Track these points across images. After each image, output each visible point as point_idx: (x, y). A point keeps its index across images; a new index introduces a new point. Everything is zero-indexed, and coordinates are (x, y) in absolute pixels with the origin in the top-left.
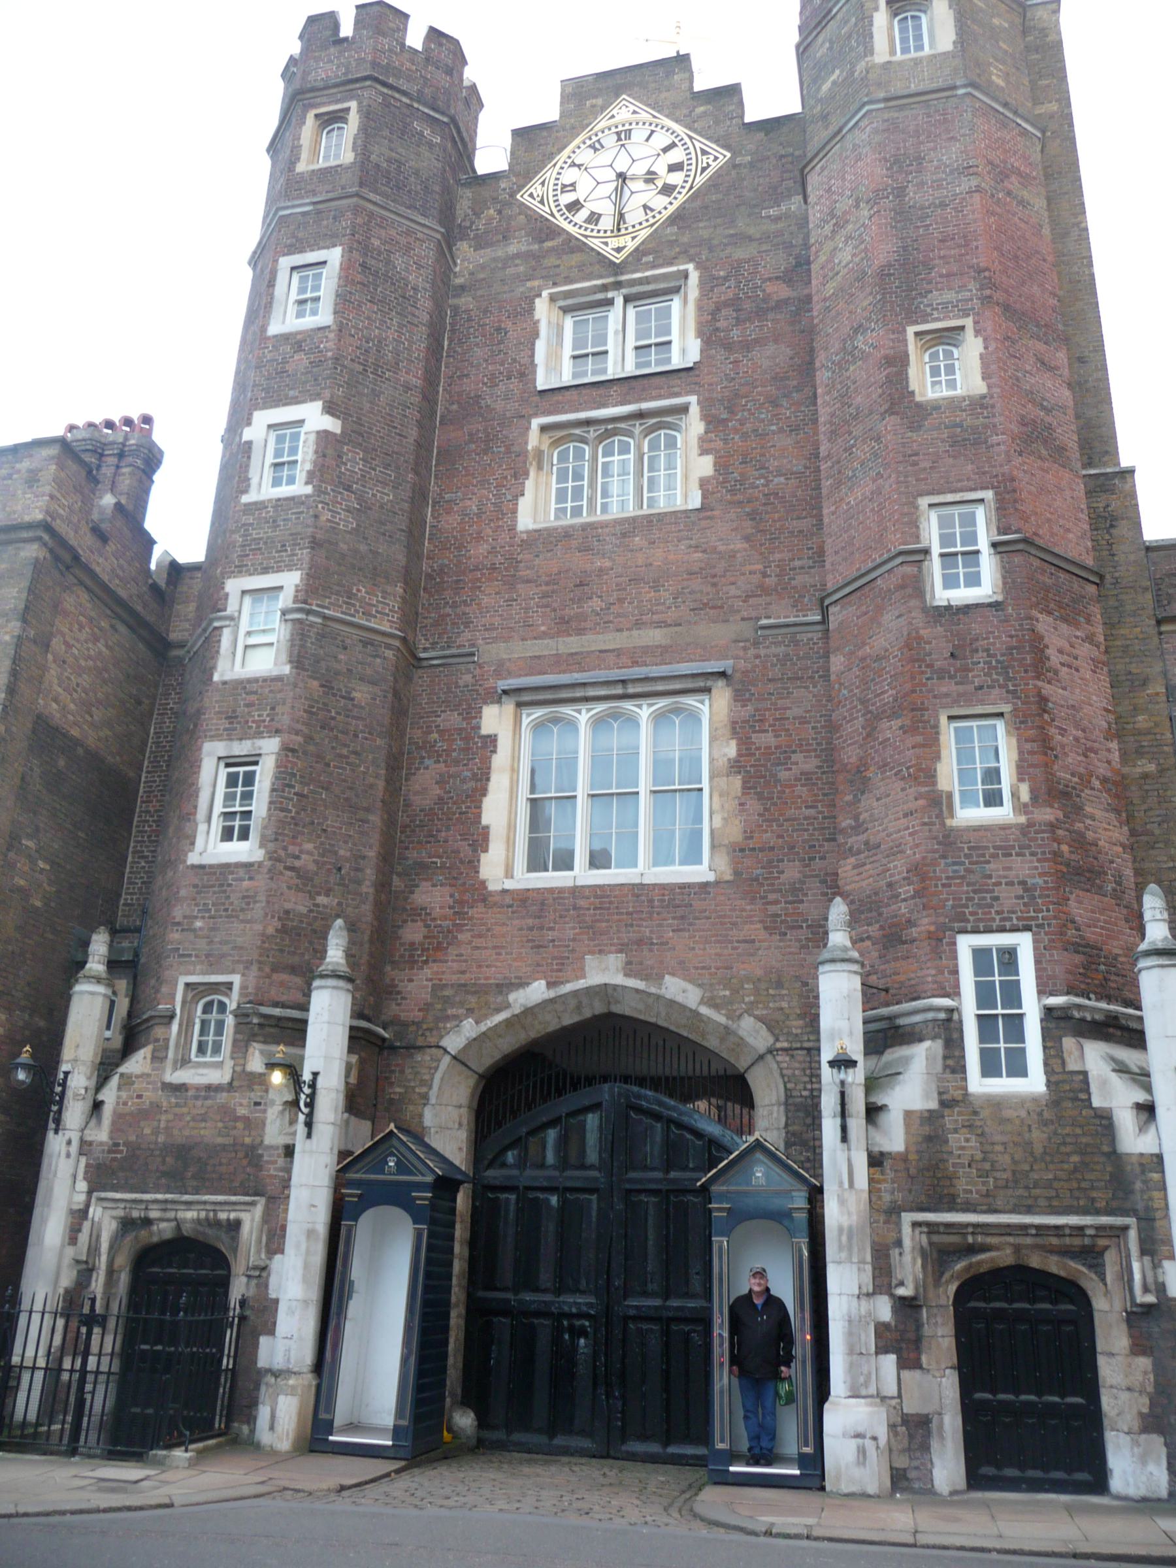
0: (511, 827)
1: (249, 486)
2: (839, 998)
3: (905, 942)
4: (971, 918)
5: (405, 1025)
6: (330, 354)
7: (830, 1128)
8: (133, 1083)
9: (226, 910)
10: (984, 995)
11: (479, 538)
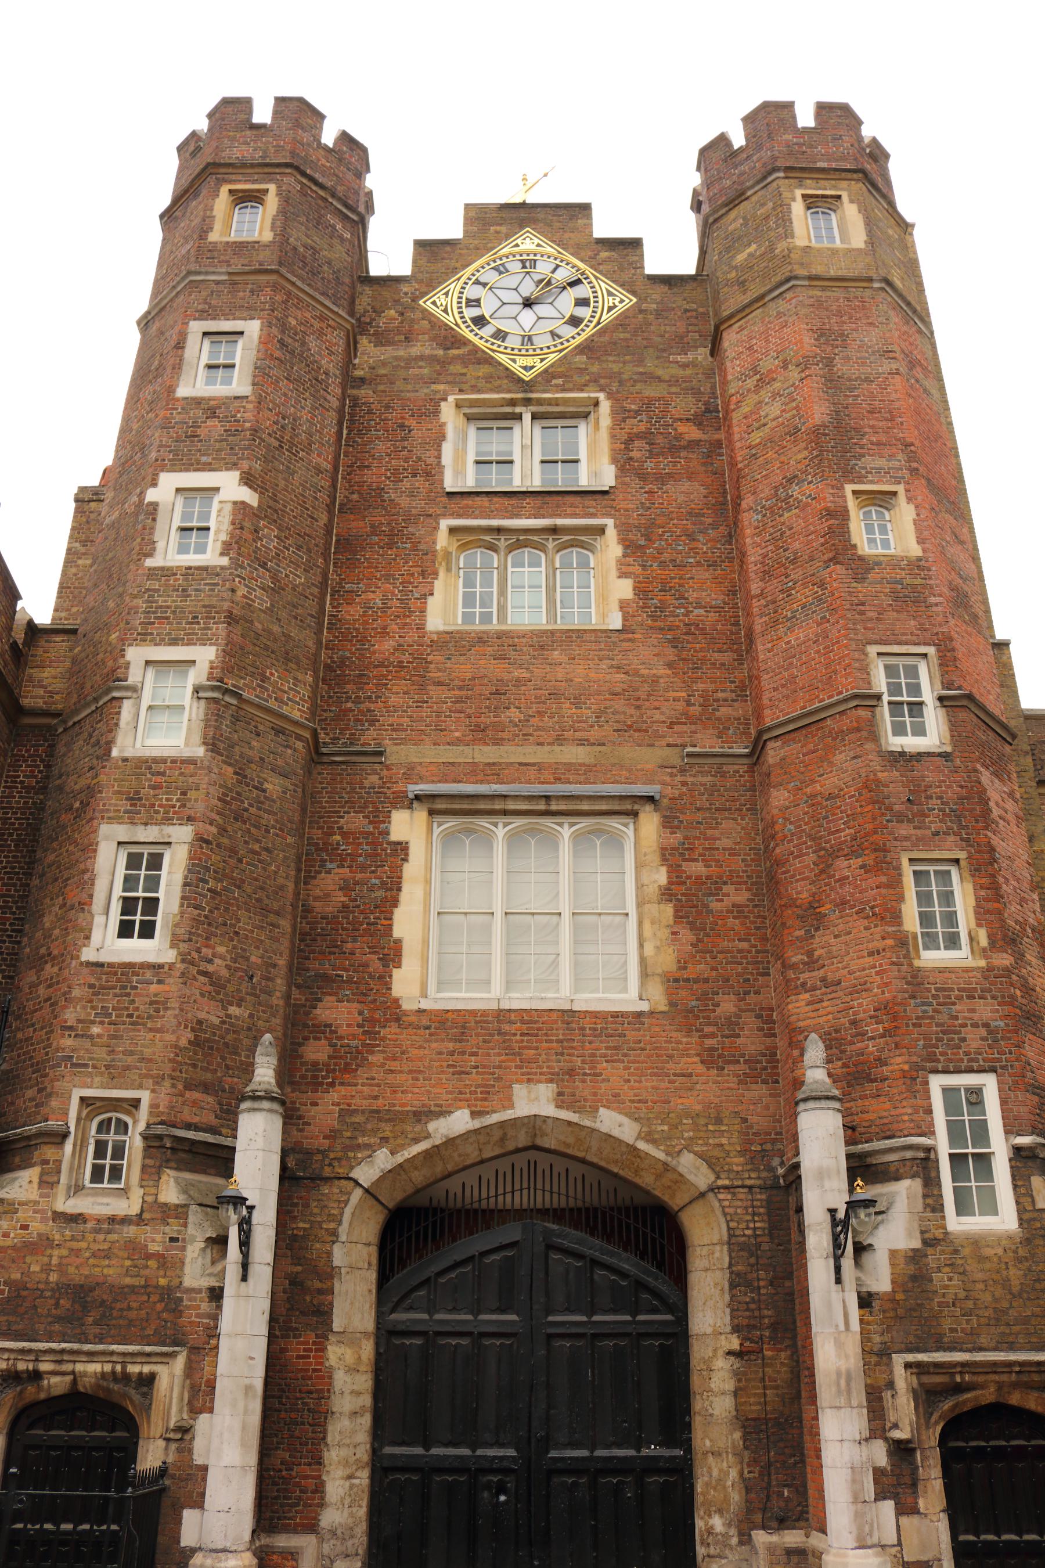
0: (426, 942)
1: (154, 549)
3: (875, 1080)
4: (942, 1058)
5: (309, 1153)
6: (248, 425)
8: (16, 1211)
9: (130, 1016)
10: (955, 1132)
11: (384, 632)
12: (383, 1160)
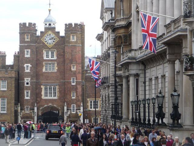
2: (65, 108)
7: (65, 115)
12: (42, 108)
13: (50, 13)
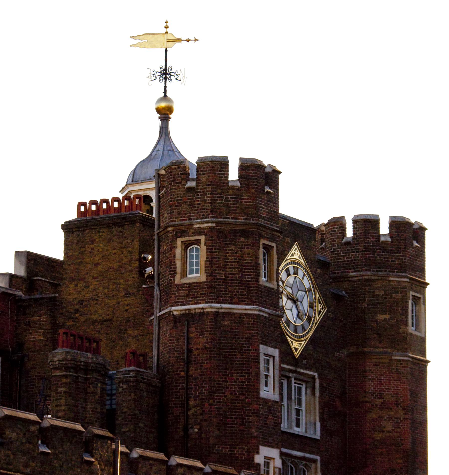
13: (164, 132)
